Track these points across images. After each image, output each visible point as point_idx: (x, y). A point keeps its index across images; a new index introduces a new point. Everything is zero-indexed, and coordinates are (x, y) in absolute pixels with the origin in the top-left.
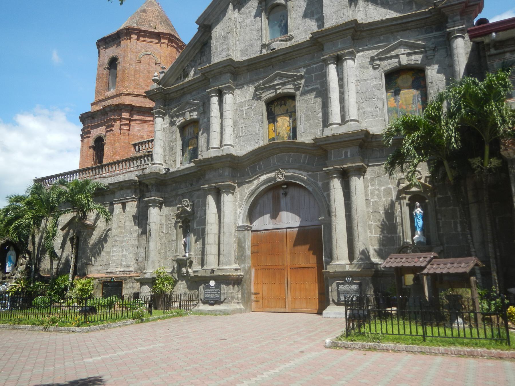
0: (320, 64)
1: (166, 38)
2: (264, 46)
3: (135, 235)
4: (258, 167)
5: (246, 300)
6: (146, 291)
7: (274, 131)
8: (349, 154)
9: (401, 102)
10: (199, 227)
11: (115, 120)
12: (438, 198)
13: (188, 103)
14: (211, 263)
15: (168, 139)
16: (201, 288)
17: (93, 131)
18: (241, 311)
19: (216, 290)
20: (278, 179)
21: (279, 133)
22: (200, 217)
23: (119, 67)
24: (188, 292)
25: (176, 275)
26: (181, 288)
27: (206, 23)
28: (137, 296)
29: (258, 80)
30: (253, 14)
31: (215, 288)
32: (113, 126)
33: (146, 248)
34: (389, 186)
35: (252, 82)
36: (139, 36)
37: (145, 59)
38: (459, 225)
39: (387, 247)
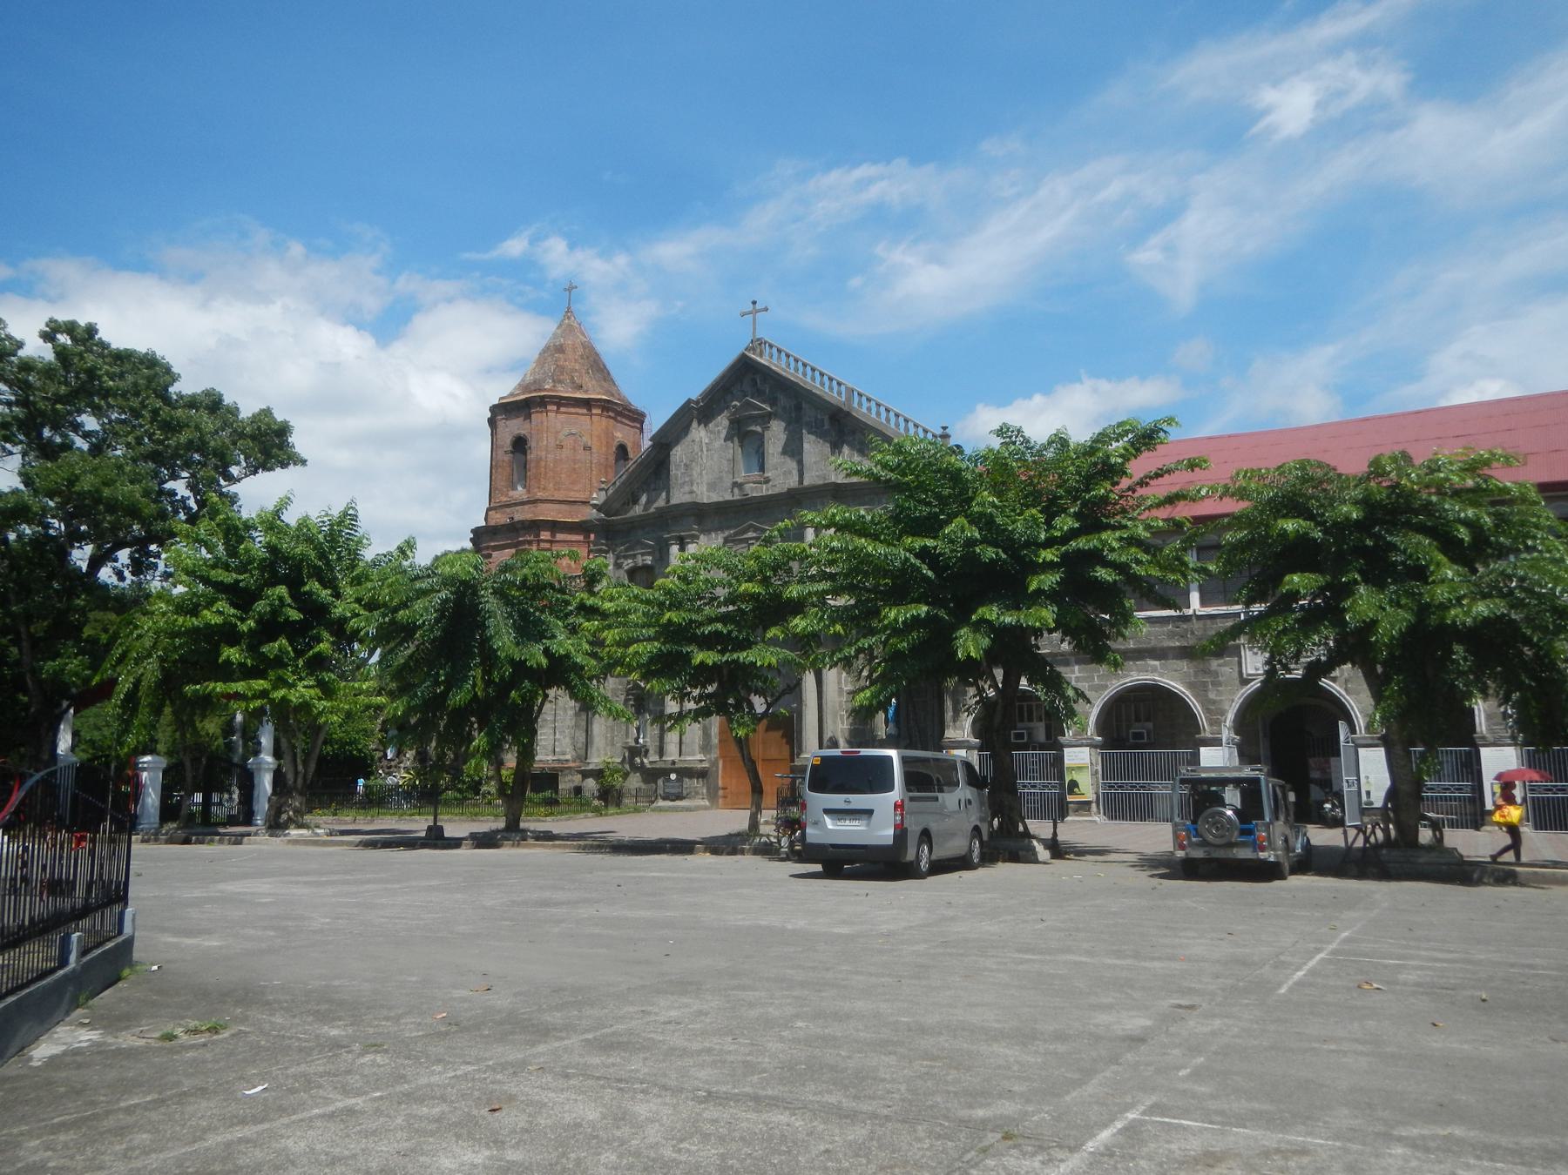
2: (735, 484)
3: (571, 713)
5: (712, 796)
6: (591, 784)
11: (530, 543)
13: (639, 543)
14: (672, 753)
16: (660, 782)
17: (495, 554)
18: (706, 808)
26: (635, 782)
28: (578, 790)
29: (728, 528)
30: (723, 435)
33: (588, 732)
35: (721, 529)
36: (559, 405)
37: (568, 443)
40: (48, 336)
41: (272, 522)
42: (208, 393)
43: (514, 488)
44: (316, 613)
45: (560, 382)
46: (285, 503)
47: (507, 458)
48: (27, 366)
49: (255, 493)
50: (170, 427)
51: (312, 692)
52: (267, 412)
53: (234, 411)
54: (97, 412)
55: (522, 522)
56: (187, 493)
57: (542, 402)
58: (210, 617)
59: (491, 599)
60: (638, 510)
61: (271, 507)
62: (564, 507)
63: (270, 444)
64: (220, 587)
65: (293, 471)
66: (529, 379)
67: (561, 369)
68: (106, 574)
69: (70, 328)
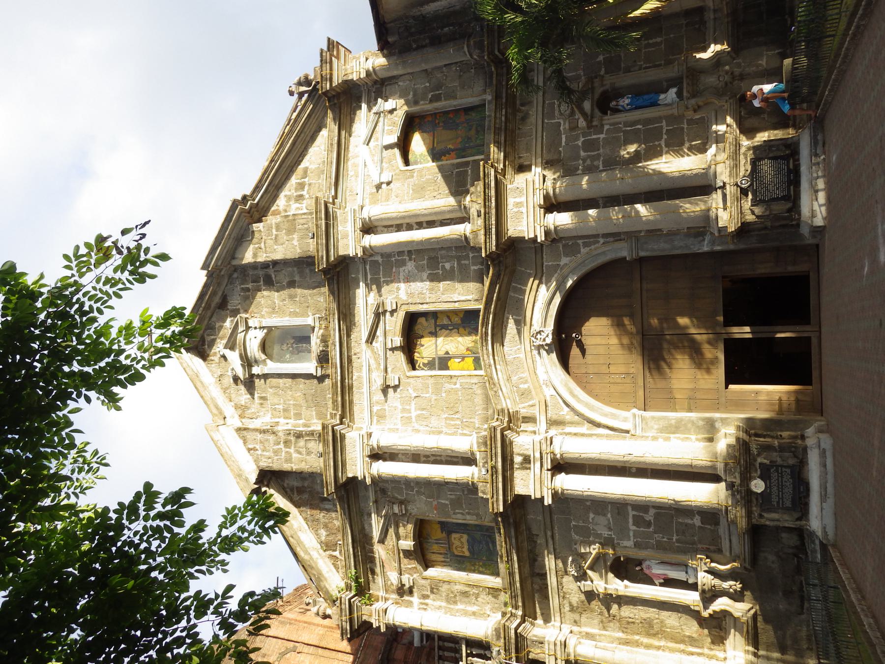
0: (368, 267)
4: (522, 386)
7: (463, 358)
8: (518, 200)
9: (450, 146)
10: (631, 534)
12: (606, 73)
15: (444, 604)
19: (774, 476)
20: (549, 340)
21: (468, 349)
22: (610, 529)
27: (253, 477)
31: (770, 478)
34: (580, 144)
38: (651, 41)
39: (686, 139)
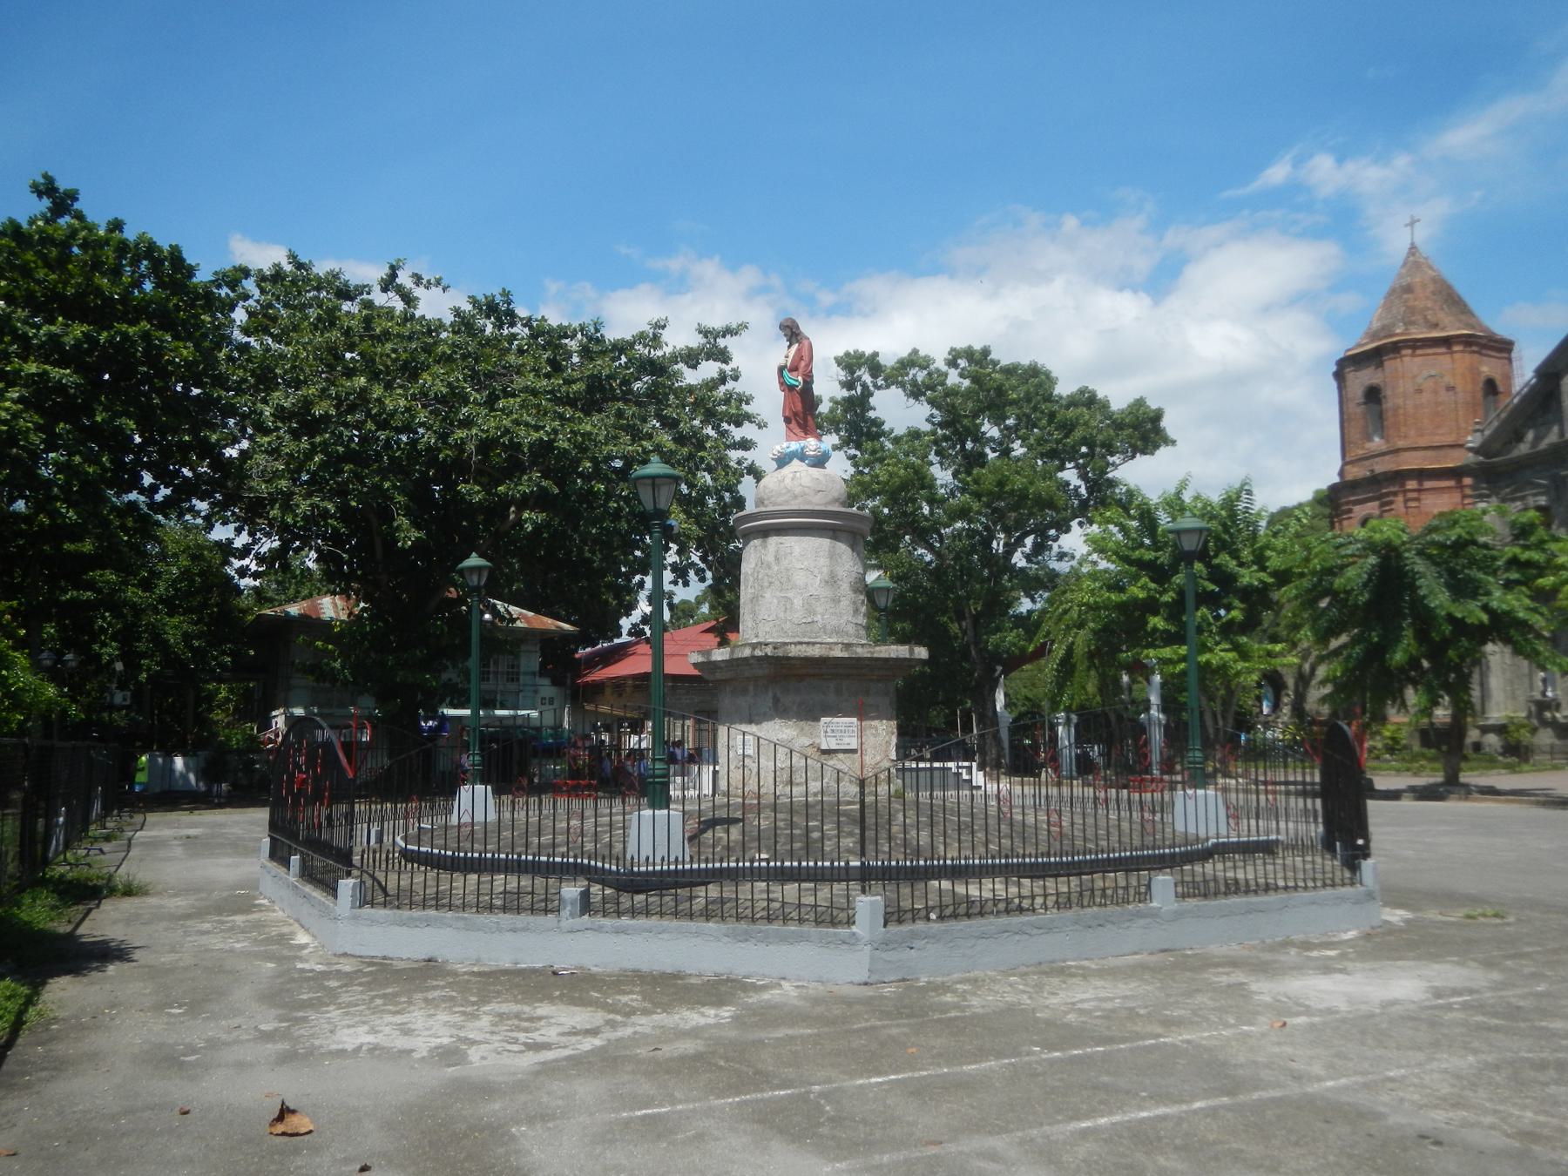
1: (1459, 343)
6: (1492, 739)
11: (1395, 494)
17: (1356, 508)
23: (1388, 405)
24: (1557, 742)
25: (1535, 722)
32: (1391, 503)
36: (1414, 348)
40: (952, 363)
41: (1175, 505)
42: (1082, 391)
43: (1370, 439)
44: (1225, 580)
45: (1413, 323)
46: (1183, 485)
47: (1359, 410)
48: (952, 392)
49: (1141, 475)
50: (1068, 428)
51: (1231, 655)
52: (1140, 403)
53: (1105, 405)
54: (998, 420)
55: (1385, 473)
56: (1079, 482)
57: (1395, 348)
58: (1137, 592)
59: (1418, 560)
60: (1523, 449)
61: (1173, 491)
62: (1429, 453)
63: (1144, 430)
64: (1142, 565)
65: (1163, 452)
66: (1376, 325)
67: (1412, 310)
68: (1018, 560)
69: (969, 354)
